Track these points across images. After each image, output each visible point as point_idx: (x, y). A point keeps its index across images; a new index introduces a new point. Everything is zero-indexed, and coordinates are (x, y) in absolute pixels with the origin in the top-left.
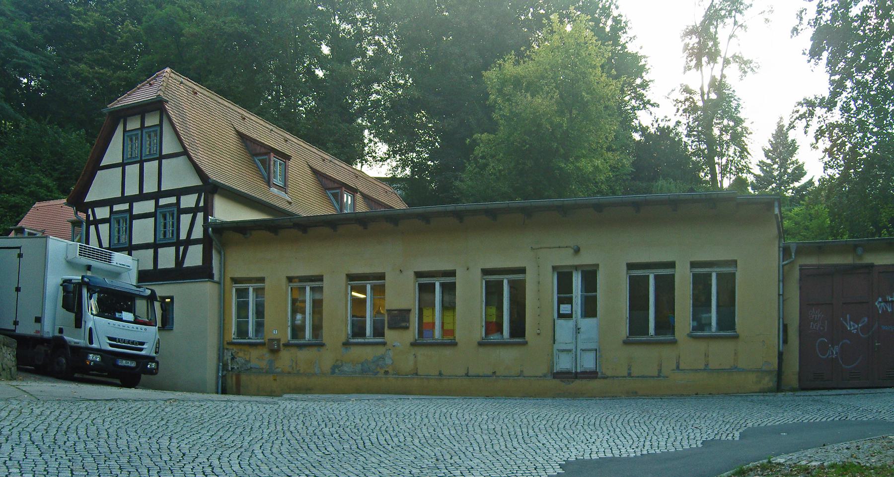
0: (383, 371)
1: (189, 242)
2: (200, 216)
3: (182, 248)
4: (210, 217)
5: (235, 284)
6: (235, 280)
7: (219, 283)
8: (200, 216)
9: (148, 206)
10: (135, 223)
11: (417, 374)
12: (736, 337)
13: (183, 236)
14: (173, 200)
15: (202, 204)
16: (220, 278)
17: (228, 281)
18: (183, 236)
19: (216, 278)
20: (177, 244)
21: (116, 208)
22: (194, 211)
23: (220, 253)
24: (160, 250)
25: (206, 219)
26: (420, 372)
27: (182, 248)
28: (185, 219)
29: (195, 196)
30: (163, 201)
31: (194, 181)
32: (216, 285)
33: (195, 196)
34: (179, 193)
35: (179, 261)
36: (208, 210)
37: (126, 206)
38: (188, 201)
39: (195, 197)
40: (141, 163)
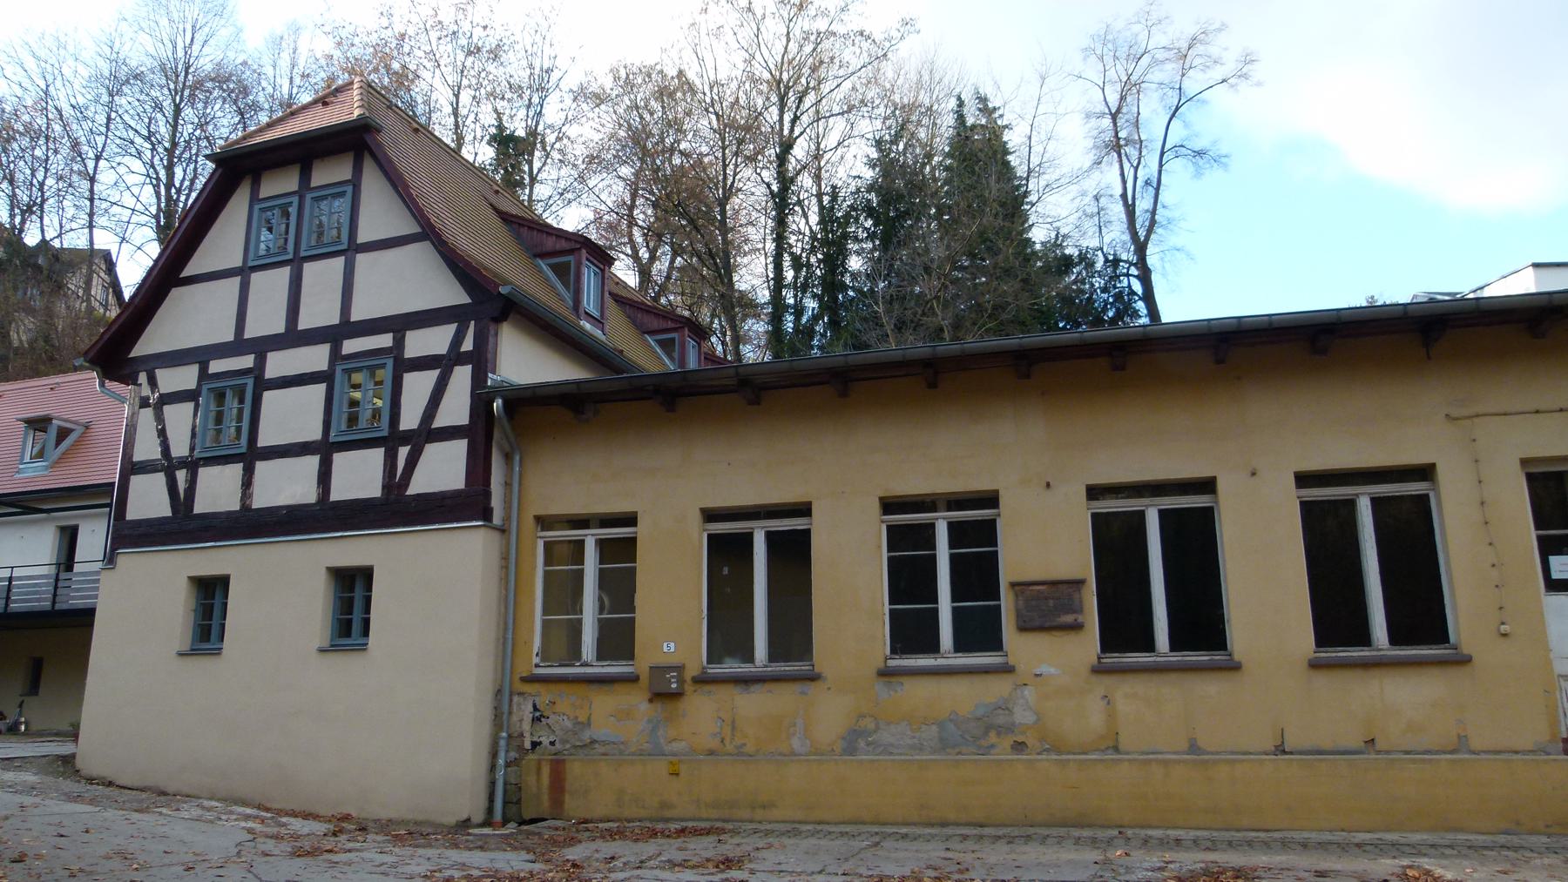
0: (1007, 742)
1: (428, 433)
2: (462, 377)
3: (403, 452)
4: (490, 375)
5: (542, 530)
6: (544, 522)
7: (502, 530)
8: (462, 377)
9: (316, 358)
10: (268, 396)
11: (1116, 749)
12: (1235, 667)
13: (410, 419)
14: (385, 340)
15: (468, 345)
16: (507, 518)
17: (529, 522)
18: (410, 419)
19: (497, 519)
20: (391, 440)
21: (216, 366)
22: (443, 364)
23: (508, 457)
24: (339, 459)
25: (478, 379)
26: (1124, 743)
27: (403, 452)
28: (418, 386)
29: (451, 329)
30: (351, 346)
31: (452, 294)
32: (495, 536)
33: (451, 329)
34: (400, 324)
35: (395, 483)
36: (481, 361)
37: (247, 361)
38: (430, 341)
39: (449, 330)
40: (297, 263)
